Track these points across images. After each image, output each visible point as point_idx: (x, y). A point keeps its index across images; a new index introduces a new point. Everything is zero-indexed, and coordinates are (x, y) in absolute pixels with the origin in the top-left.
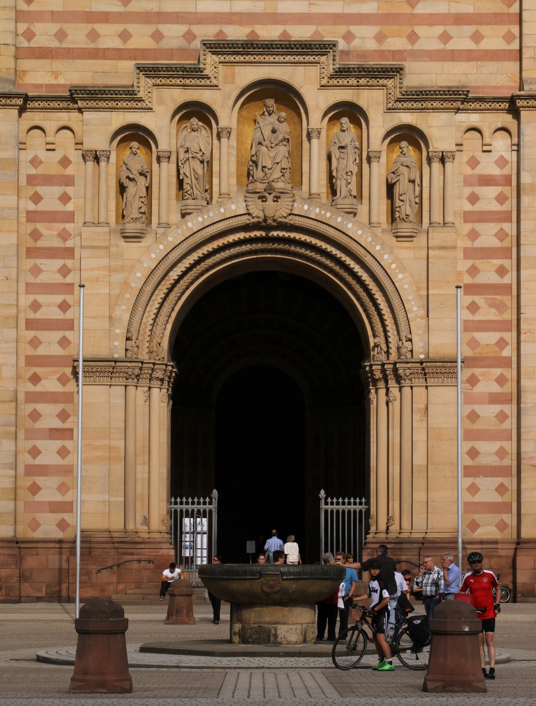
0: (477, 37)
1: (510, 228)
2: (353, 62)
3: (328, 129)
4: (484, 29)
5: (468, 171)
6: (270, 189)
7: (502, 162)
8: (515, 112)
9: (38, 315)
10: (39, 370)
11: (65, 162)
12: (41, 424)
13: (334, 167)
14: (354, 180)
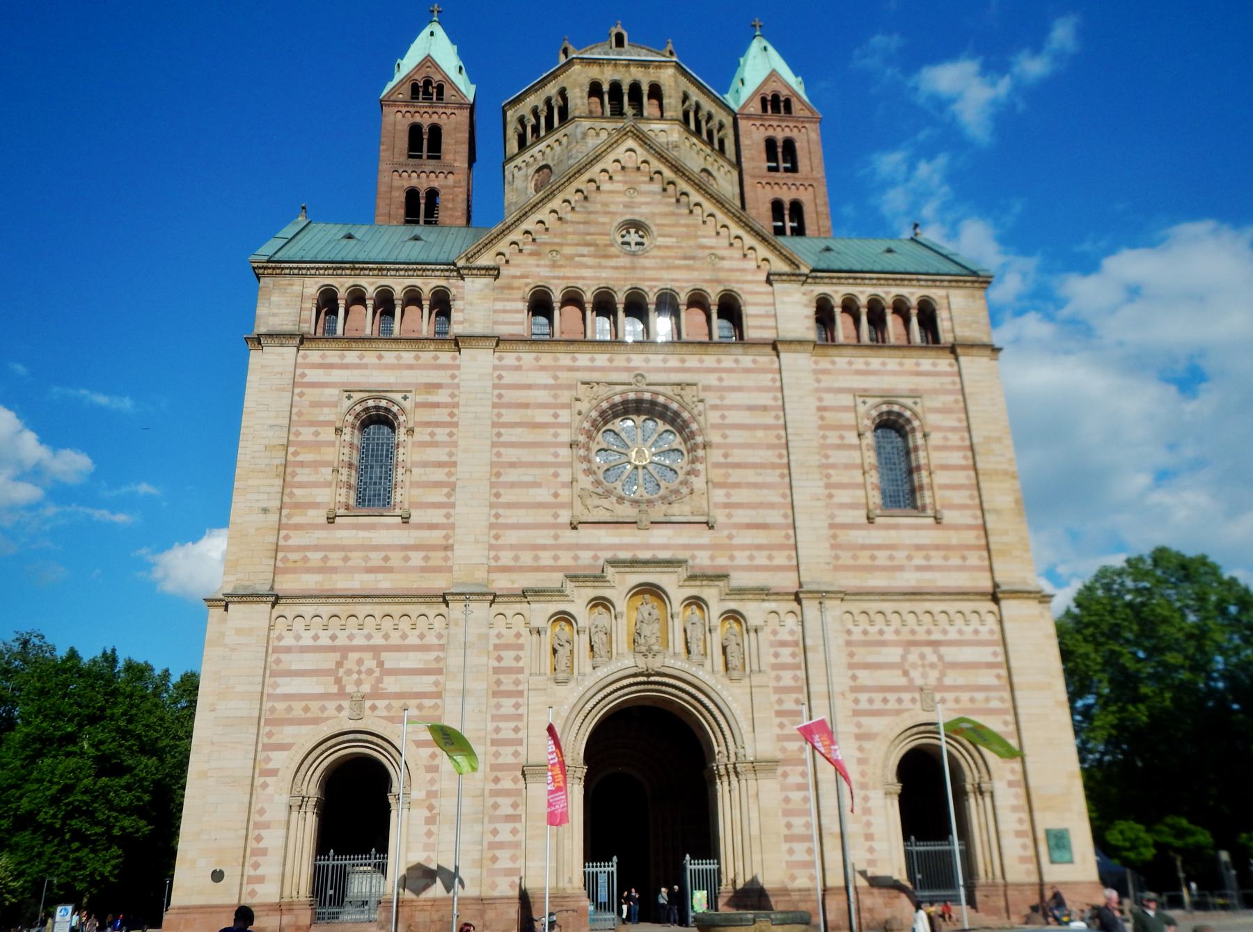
0: (770, 558)
1: (801, 674)
2: (698, 572)
3: (684, 612)
4: (775, 553)
5: (772, 638)
6: (650, 650)
7: (792, 632)
8: (798, 600)
9: (500, 736)
10: (499, 774)
11: (518, 635)
12: (500, 812)
13: (689, 636)
14: (701, 644)
